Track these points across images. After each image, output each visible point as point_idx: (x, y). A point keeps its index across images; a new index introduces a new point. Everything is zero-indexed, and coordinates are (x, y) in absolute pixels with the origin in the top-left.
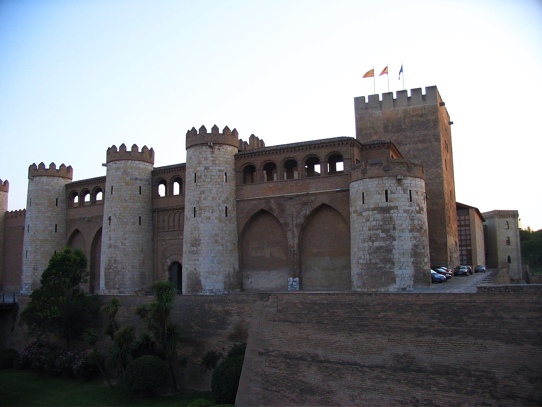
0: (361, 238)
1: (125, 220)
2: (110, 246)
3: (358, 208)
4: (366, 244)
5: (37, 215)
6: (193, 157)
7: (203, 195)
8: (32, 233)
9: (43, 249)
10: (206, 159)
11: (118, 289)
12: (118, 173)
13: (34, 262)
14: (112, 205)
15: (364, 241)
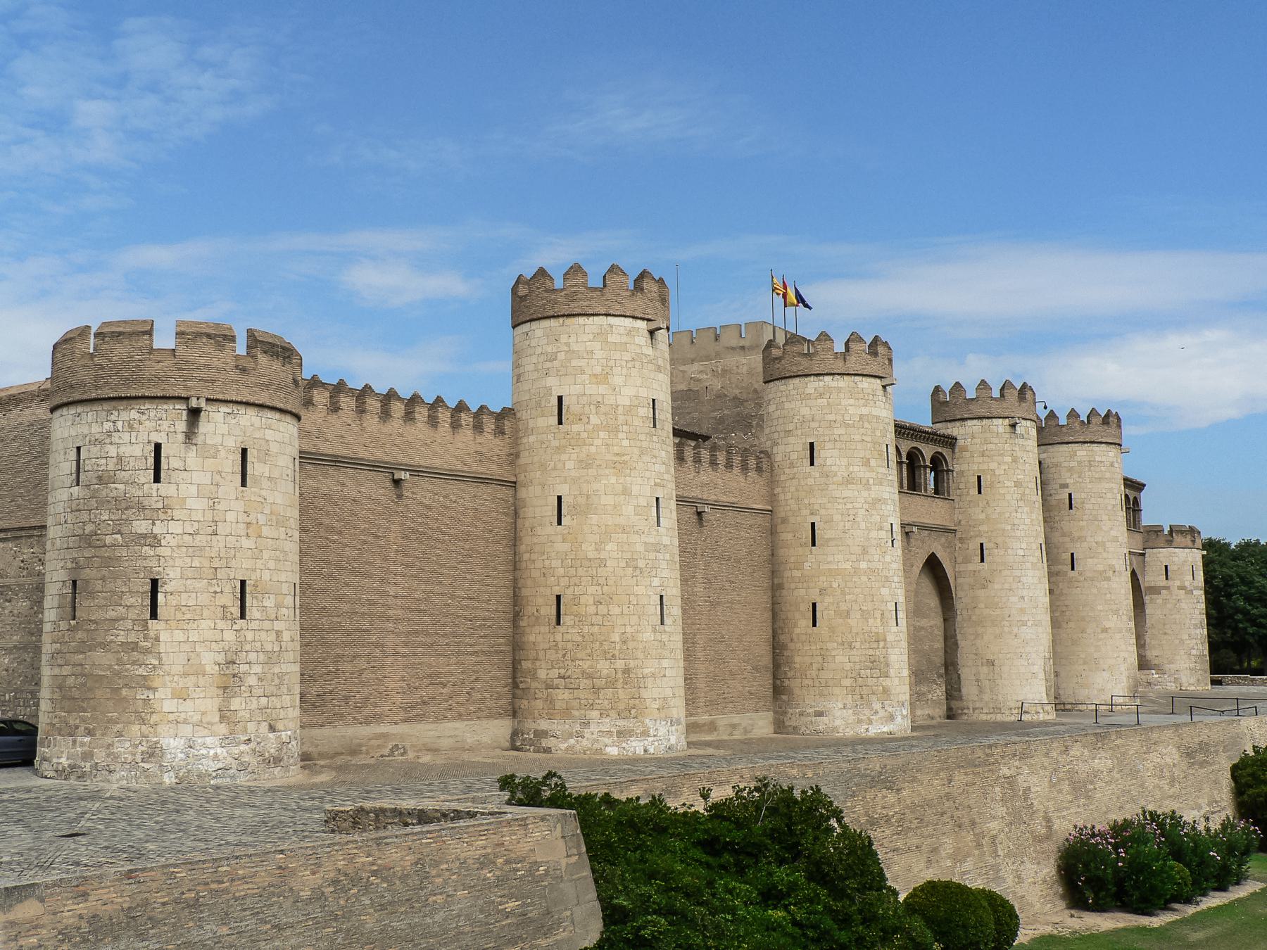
3: (1187, 584)
4: (1198, 631)
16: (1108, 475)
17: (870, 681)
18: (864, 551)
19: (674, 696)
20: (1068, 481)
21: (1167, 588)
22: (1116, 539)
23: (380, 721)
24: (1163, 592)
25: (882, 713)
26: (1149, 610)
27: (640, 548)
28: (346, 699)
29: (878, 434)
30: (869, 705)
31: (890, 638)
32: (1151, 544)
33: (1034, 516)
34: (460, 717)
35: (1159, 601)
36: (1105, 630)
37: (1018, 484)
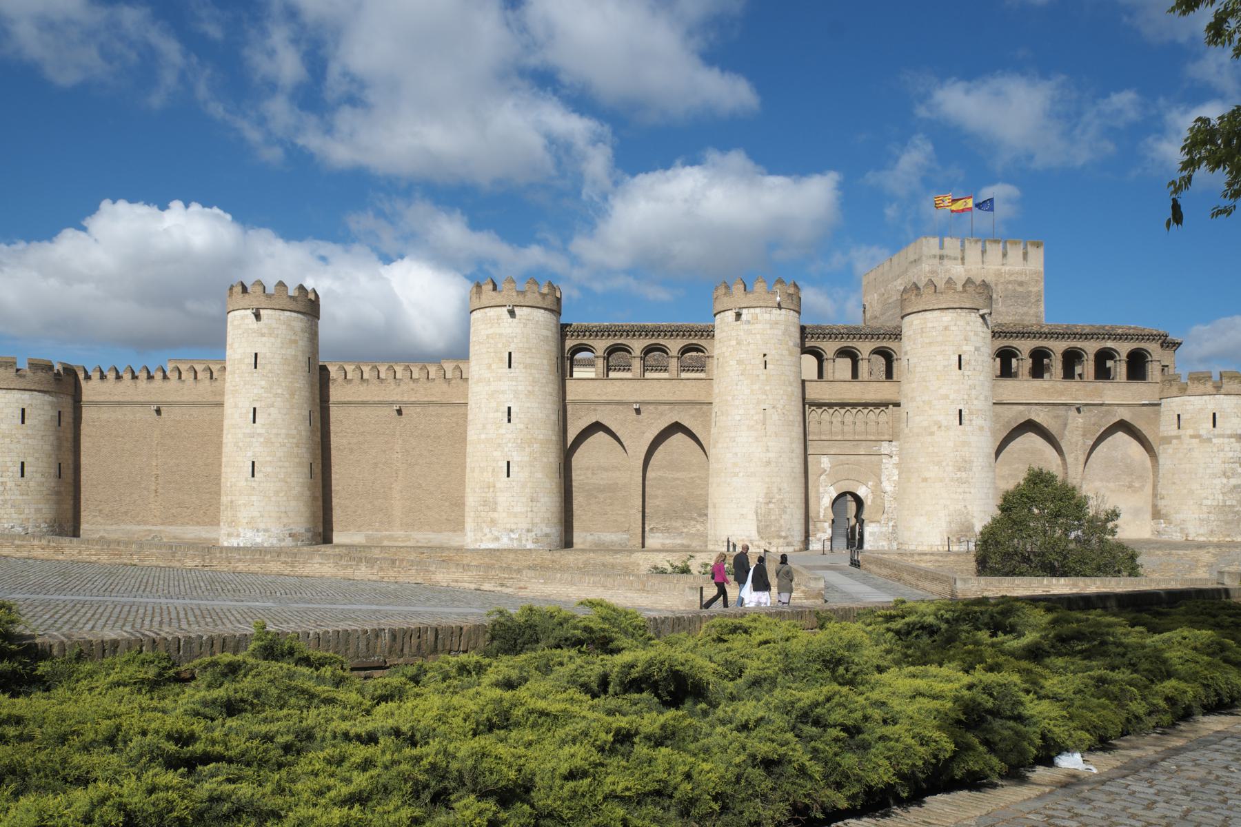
0: (1208, 471)
1: (791, 418)
2: (769, 463)
3: (1202, 432)
4: (1217, 481)
5: (530, 388)
6: (953, 328)
7: (974, 392)
8: (522, 426)
9: (545, 460)
10: (976, 334)
11: (785, 538)
12: (776, 332)
13: (529, 485)
14: (768, 388)
15: (1214, 476)
16: (940, 339)
17: (483, 514)
18: (484, 427)
19: (262, 516)
20: (908, 348)
21: (1178, 437)
22: (946, 397)
23: (146, 523)
24: (1174, 441)
25: (489, 535)
26: (1161, 461)
27: (240, 436)
28: (126, 513)
29: (500, 345)
30: (481, 529)
31: (498, 485)
32: (1165, 395)
33: (756, 387)
34: (198, 523)
35: (1170, 451)
36: (925, 480)
37: (740, 362)
